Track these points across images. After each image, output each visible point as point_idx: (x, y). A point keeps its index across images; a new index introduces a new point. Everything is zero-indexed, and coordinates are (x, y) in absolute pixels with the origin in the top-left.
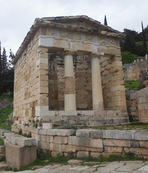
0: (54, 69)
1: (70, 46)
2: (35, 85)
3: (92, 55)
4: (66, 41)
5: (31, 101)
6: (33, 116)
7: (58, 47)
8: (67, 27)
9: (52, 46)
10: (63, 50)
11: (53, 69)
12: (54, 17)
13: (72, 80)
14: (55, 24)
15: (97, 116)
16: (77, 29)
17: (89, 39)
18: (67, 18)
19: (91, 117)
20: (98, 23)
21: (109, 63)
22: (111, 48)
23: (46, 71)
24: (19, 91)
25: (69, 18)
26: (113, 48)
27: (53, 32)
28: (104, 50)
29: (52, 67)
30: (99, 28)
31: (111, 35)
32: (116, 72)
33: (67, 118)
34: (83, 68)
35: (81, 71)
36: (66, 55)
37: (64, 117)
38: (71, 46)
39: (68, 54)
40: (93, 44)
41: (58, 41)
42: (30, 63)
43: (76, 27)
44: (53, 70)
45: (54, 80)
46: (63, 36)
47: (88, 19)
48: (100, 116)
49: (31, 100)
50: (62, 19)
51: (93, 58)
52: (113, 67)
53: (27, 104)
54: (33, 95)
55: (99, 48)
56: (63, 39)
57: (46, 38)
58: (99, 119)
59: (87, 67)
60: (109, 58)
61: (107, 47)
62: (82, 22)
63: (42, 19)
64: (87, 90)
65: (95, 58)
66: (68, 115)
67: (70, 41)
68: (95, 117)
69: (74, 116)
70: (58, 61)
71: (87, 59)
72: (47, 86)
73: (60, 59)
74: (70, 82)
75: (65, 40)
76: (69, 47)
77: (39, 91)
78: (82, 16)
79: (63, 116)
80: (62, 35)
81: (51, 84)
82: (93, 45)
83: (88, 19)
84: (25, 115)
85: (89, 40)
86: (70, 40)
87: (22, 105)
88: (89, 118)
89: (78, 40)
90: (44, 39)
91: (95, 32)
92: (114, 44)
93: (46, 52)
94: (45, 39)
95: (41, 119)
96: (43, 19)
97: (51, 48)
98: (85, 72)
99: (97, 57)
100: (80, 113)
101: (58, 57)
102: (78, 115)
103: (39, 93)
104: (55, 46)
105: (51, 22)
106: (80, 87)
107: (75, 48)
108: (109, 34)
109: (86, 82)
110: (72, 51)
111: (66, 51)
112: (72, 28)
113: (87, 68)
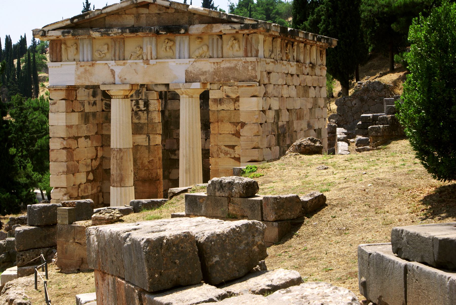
0: (145, 108)
9: (73, 84)
11: (143, 109)
12: (67, 20)
13: (118, 157)
18: (99, 12)
25: (103, 11)
28: (204, 73)
29: (141, 103)
30: (194, 14)
34: (228, 96)
35: (220, 108)
38: (116, 76)
41: (86, 71)
44: (144, 110)
45: (145, 136)
50: (87, 19)
55: (190, 69)
56: (98, 62)
61: (214, 63)
62: (148, 8)
63: (45, 29)
64: (237, 156)
72: (64, 172)
74: (115, 161)
81: (138, 145)
82: (174, 64)
96: (46, 29)
98: (233, 108)
105: (63, 33)
106: (218, 150)
107: (125, 79)
109: (233, 134)
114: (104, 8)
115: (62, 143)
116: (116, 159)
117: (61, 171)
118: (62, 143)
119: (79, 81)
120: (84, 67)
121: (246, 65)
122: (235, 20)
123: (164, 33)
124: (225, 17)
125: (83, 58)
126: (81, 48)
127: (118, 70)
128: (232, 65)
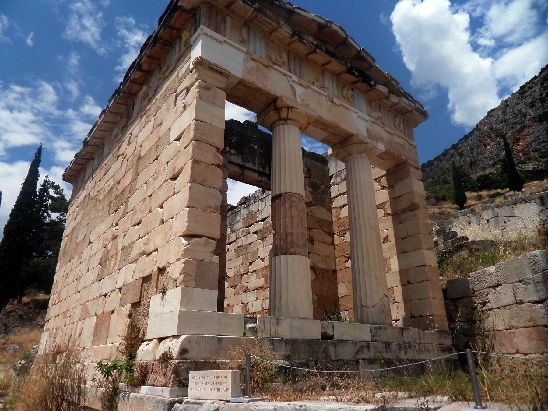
1: (295, 95)
2: (159, 208)
3: (351, 146)
4: (284, 77)
5: (130, 280)
6: (134, 338)
7: (260, 85)
8: (289, 34)
10: (269, 105)
14: (255, 9)
15: (381, 346)
16: (318, 51)
17: (346, 96)
18: (291, 7)
19: (362, 347)
20: (369, 59)
21: (383, 188)
22: (397, 140)
23: (215, 150)
24: (76, 257)
25: (296, 10)
26: (401, 141)
27: (245, 36)
28: (381, 139)
31: (397, 103)
32: (411, 211)
33: (289, 349)
36: (282, 122)
37: (277, 344)
39: (286, 119)
40: (357, 113)
42: (138, 148)
43: (315, 43)
46: (276, 60)
47: (345, 36)
48: (388, 345)
49: (128, 275)
51: (350, 155)
52: (396, 196)
53: (105, 296)
54: (143, 253)
55: (370, 128)
56: (276, 67)
57: (221, 42)
58: (384, 355)
59: (311, 199)
60: (384, 173)
61: (388, 132)
65: (359, 156)
66: (287, 335)
67: (297, 80)
68: (376, 348)
69: (310, 342)
70: (232, 165)
71: (309, 177)
72: (216, 208)
73: (237, 159)
75: (281, 72)
76: (293, 98)
77: (180, 224)
78: (330, 22)
79: (273, 340)
80: (273, 57)
82: (355, 115)
83: (346, 39)
84: (91, 339)
85: (345, 98)
86: (294, 78)
87: (83, 302)
88: (357, 353)
89: (316, 86)
90: (215, 42)
91: (363, 81)
92: (401, 131)
93: (220, 88)
94: (219, 44)
95: (183, 351)
97: (234, 87)
99: (368, 155)
100: (330, 332)
101: (233, 151)
102: (322, 339)
103: (181, 234)
104: (251, 79)
108: (394, 99)
110: (304, 113)
111: (281, 108)
112: (305, 41)
113: (309, 202)
114: (299, 8)
115: (217, 156)
116: (297, 210)
117: (212, 204)
118: (215, 156)
119: (249, 76)
120: (257, 63)
121: (411, 147)
122: (410, 98)
123: (357, 74)
124: (402, 91)
125: (255, 51)
126: (252, 38)
127: (299, 90)
128: (401, 141)
